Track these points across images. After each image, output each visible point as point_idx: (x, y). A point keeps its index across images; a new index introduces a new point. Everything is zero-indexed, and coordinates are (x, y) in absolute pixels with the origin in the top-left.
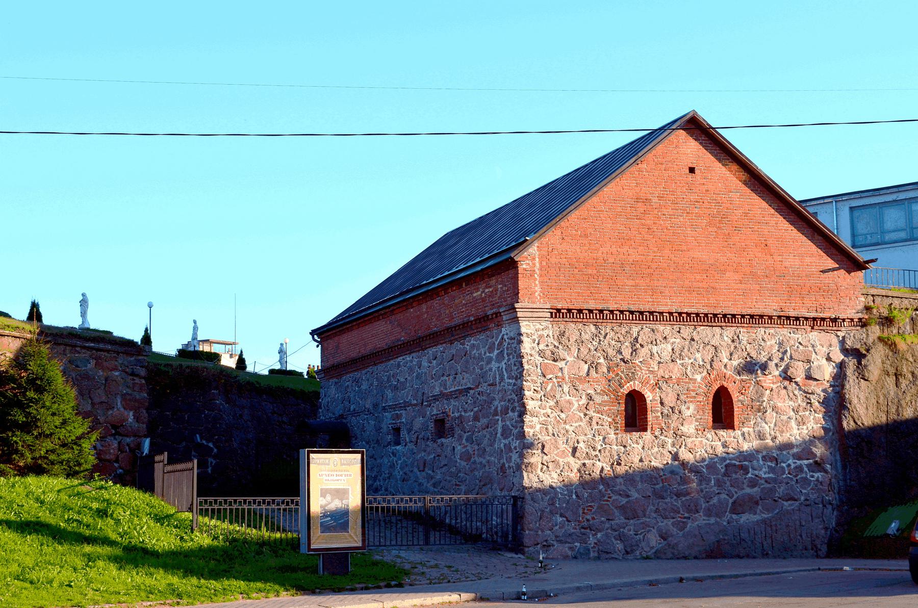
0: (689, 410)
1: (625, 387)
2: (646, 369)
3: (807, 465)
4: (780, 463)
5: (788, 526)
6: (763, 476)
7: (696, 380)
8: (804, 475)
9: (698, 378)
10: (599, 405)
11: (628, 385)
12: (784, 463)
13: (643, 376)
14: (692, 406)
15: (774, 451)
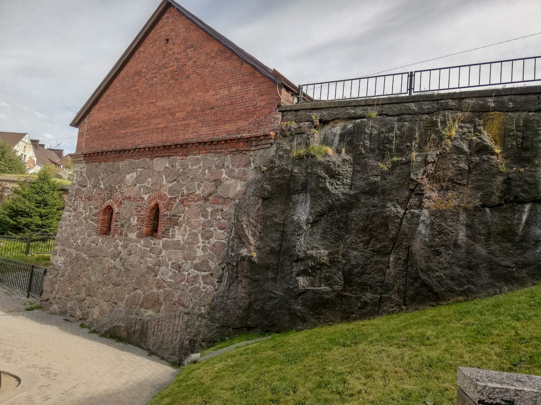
0: (134, 221)
2: (119, 191)
3: (204, 277)
4: (183, 271)
7: (144, 198)
8: (197, 285)
9: (146, 197)
10: (93, 215)
12: (187, 271)
15: (180, 260)
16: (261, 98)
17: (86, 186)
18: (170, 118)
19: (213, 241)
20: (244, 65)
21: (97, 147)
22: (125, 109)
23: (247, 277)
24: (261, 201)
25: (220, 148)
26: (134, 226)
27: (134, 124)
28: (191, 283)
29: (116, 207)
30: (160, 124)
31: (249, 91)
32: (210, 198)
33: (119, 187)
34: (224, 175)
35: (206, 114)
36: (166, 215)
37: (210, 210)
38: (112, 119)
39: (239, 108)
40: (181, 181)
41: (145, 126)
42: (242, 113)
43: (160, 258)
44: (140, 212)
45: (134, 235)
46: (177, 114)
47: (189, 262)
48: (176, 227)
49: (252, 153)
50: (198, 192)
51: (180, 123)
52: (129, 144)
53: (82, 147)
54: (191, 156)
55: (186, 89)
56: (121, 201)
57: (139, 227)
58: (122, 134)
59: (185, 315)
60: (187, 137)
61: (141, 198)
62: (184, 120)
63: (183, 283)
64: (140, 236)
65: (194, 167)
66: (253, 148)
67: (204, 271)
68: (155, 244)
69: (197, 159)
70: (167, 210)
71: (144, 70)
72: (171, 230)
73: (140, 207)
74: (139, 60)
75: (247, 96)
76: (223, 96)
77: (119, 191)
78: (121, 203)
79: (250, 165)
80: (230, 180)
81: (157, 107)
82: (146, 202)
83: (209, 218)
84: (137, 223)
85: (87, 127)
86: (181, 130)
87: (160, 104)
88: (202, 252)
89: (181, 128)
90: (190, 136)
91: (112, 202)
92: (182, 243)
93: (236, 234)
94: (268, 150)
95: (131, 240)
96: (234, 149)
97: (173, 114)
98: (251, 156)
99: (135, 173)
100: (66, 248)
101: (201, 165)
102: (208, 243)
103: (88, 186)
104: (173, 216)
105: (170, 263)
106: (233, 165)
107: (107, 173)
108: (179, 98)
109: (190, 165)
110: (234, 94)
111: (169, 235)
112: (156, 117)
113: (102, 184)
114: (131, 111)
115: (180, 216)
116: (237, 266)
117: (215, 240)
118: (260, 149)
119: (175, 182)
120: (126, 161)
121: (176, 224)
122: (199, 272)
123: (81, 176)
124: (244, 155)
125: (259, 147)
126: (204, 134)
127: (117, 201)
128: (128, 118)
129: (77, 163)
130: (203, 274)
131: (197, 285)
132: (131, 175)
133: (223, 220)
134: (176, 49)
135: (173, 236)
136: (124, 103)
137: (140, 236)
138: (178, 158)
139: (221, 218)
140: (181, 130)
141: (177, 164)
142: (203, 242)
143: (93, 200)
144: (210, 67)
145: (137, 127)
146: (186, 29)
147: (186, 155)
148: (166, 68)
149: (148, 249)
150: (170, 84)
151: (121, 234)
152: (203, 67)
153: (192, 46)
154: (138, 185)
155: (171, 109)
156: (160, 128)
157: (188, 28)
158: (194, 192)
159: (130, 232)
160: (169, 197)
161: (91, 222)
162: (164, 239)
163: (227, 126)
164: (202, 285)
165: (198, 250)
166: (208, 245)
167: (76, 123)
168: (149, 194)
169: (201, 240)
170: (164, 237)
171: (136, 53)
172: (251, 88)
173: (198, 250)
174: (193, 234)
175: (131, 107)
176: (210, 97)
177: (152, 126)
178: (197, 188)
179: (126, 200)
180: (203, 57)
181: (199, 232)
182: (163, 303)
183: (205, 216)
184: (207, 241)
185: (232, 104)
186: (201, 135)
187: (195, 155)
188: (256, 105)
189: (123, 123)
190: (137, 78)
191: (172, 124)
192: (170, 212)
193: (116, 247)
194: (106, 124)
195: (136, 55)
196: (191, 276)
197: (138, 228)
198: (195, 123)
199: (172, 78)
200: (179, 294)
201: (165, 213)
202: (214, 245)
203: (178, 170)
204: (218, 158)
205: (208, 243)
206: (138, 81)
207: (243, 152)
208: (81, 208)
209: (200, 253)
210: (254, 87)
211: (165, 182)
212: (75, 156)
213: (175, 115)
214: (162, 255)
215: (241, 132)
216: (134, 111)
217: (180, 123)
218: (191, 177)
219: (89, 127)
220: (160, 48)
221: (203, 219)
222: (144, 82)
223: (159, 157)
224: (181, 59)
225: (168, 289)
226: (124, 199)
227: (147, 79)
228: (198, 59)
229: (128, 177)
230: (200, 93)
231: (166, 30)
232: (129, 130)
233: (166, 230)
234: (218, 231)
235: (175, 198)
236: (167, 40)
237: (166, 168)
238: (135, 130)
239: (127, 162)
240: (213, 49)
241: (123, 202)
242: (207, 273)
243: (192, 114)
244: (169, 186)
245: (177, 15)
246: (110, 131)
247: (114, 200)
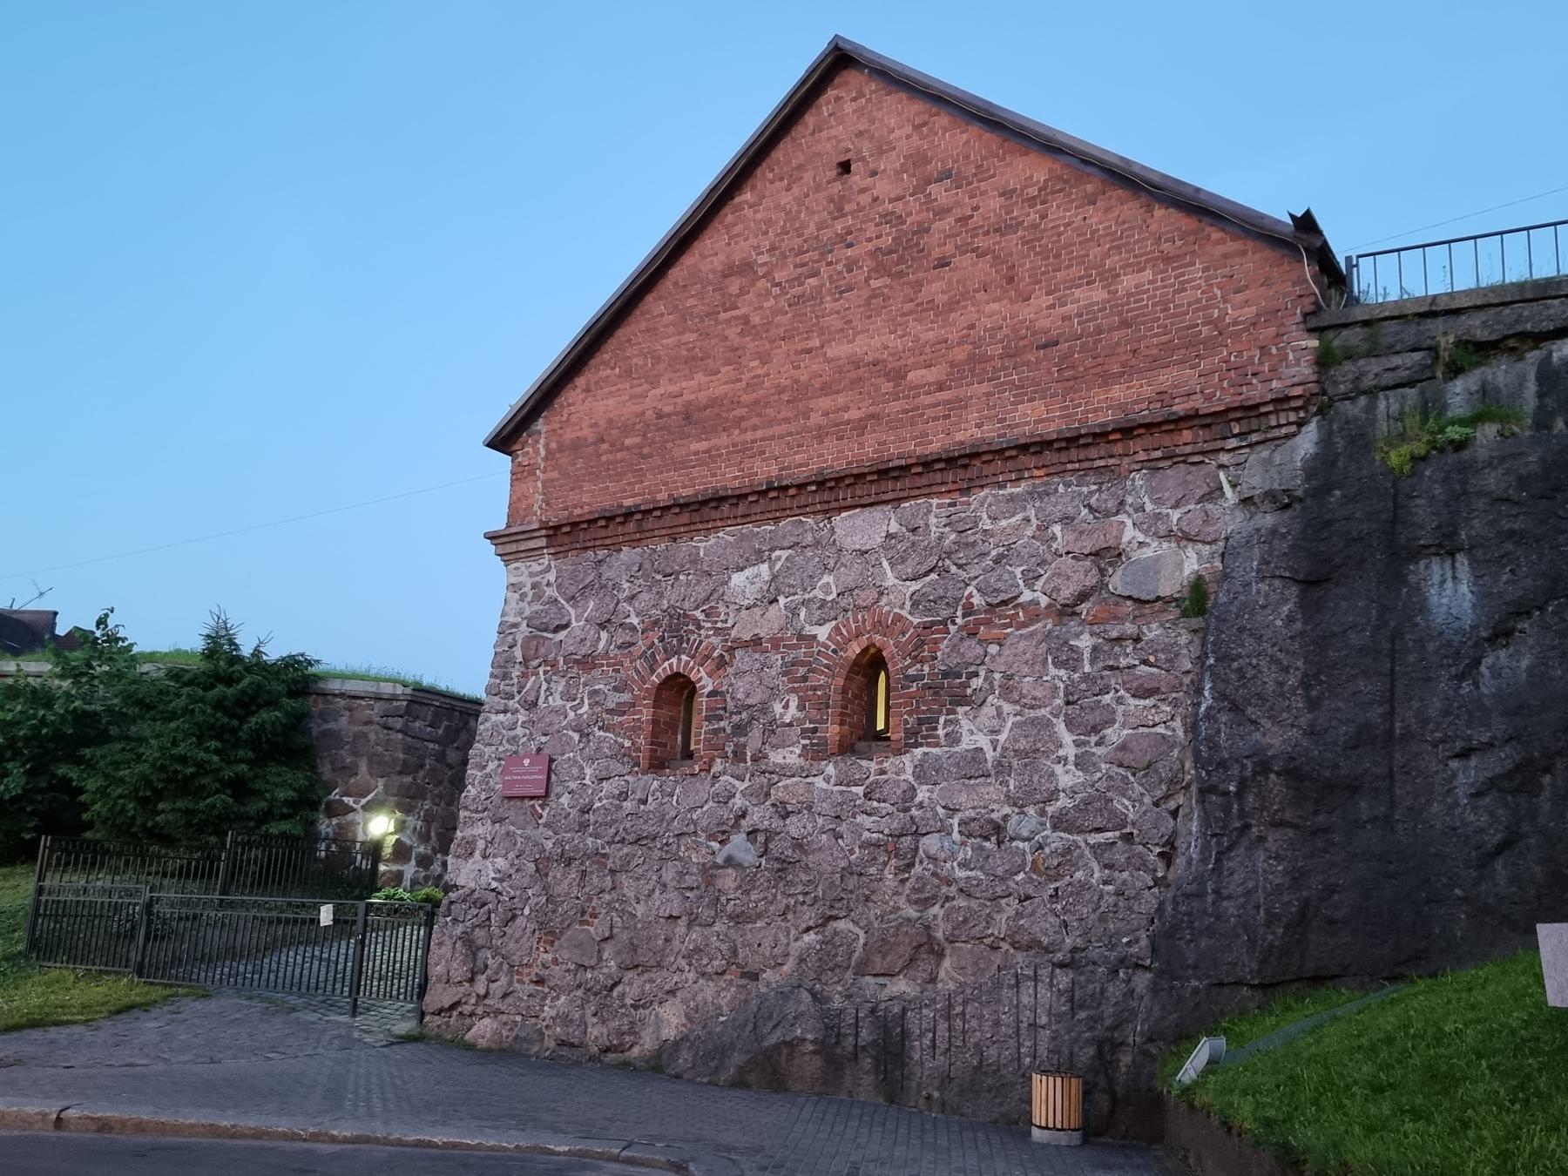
0: (788, 710)
1: (660, 670)
2: (709, 625)
4: (1012, 839)
5: (997, 1023)
6: (961, 874)
8: (1079, 875)
10: (610, 712)
11: (666, 664)
13: (701, 642)
14: (794, 704)
15: (995, 806)
16: (1239, 297)
17: (566, 626)
18: (887, 387)
19: (1114, 734)
20: (1159, 212)
21: (590, 499)
22: (700, 378)
23: (1278, 824)
24: (1294, 590)
25: (1102, 453)
26: (790, 725)
27: (742, 418)
28: (1051, 873)
29: (703, 673)
30: (846, 409)
31: (1188, 281)
32: (1084, 608)
33: (707, 615)
34: (1130, 533)
35: (1028, 364)
36: (914, 679)
37: (1085, 642)
38: (649, 413)
39: (1156, 335)
40: (953, 569)
41: (787, 420)
42: (1168, 347)
43: (914, 812)
44: (805, 679)
45: (791, 752)
46: (911, 375)
47: (1031, 810)
48: (960, 710)
49: (1224, 458)
50: (1027, 596)
51: (929, 400)
52: (728, 477)
53: (530, 506)
54: (986, 491)
55: (941, 299)
56: (721, 656)
57: (807, 725)
58: (696, 453)
59: (1058, 971)
60: (959, 437)
61: (801, 637)
62: (941, 389)
63: (1021, 876)
64: (817, 752)
65: (1004, 523)
66: (1232, 443)
67: (1099, 830)
68: (883, 772)
69: (1012, 498)
70: (918, 660)
71: (762, 259)
72: (942, 720)
73: (803, 664)
74: (736, 230)
75: (1184, 298)
76: (1086, 307)
77: (709, 625)
78: (722, 663)
79: (1223, 494)
80: (1155, 544)
81: (830, 361)
82: (827, 647)
83: (1087, 669)
84: (799, 715)
85: (547, 446)
86: (935, 419)
87: (839, 350)
88: (1081, 773)
89: (930, 412)
90: (970, 431)
91: (687, 663)
92: (990, 755)
93: (1220, 696)
94: (1291, 443)
95: (784, 772)
96: (1158, 454)
97: (898, 376)
98: (1221, 466)
99: (764, 567)
100: (512, 828)
101: (1032, 513)
102: (1098, 744)
103: (574, 624)
104: (945, 675)
105: (955, 821)
106: (1157, 502)
107: (646, 577)
108: (914, 327)
109: (985, 516)
110: (1129, 295)
111: (938, 737)
112: (826, 390)
113: (633, 615)
114: (726, 383)
115: (976, 674)
116: (1240, 794)
117: (1126, 732)
118: (1257, 443)
119: (934, 576)
120: (721, 534)
121: (963, 700)
122: (1079, 838)
123: (538, 597)
124: (1193, 468)
125: (1254, 438)
126: (1027, 423)
127: (707, 657)
128: (714, 402)
129: (517, 560)
130: (1094, 838)
131: (1079, 875)
132: (749, 572)
133: (1143, 667)
134: (882, 188)
135: (953, 739)
136: (692, 361)
137: (817, 752)
138: (935, 501)
139: (1137, 662)
140: (935, 419)
141: (933, 520)
142: (1077, 744)
143: (602, 665)
144: (1026, 229)
145: (755, 428)
146: (917, 128)
147: (966, 491)
148: (850, 246)
149: (859, 790)
150: (874, 290)
151: (739, 756)
152: (996, 231)
153: (948, 175)
154: (782, 600)
155: (884, 361)
156: (848, 422)
157: (925, 124)
158: (1016, 598)
159: (775, 747)
160: (916, 621)
161: (601, 733)
162: (918, 752)
163: (1118, 392)
164: (1096, 875)
165: (1059, 769)
166: (1100, 751)
167: (504, 440)
168: (834, 623)
169: (1067, 738)
170: (917, 745)
171: (727, 209)
172: (1196, 272)
173: (1059, 769)
174: (1033, 722)
175: (724, 370)
176: (1039, 312)
177: (816, 418)
178: (1021, 582)
179: (739, 653)
180: (995, 203)
181: (1057, 716)
182: (948, 952)
183: (1070, 661)
184: (1094, 739)
185: (1125, 324)
186: (1017, 426)
187: (1002, 486)
188: (1221, 318)
189: (691, 418)
190: (734, 286)
191: (895, 406)
192: (932, 668)
193: (726, 799)
194: (626, 430)
195: (728, 215)
196: (1047, 850)
197: (804, 731)
198: (988, 395)
199: (880, 270)
200: (1011, 912)
201: (911, 672)
202: (1123, 747)
203: (941, 538)
204: (1094, 487)
205: (1098, 744)
206: (743, 291)
207: (1196, 459)
208: (558, 697)
209: (1067, 777)
210: (1205, 270)
211: (891, 580)
212: (513, 538)
213: (904, 377)
214: (917, 800)
215: (1177, 401)
216: (740, 380)
217: (929, 400)
218: (994, 553)
219: (553, 445)
220: (818, 188)
221: (1062, 673)
222: (768, 292)
223: (855, 507)
224: (909, 214)
225: (961, 902)
226: (731, 650)
227: (779, 284)
228: (976, 209)
229: (738, 579)
230: (995, 306)
231: (835, 137)
232: (723, 440)
233: (920, 722)
234: (1132, 701)
235: (944, 623)
236: (845, 167)
237: (889, 536)
238: (749, 436)
239: (725, 536)
240: (1031, 177)
241: (727, 658)
242: (1110, 834)
243: (972, 371)
244: (912, 589)
245: (872, 92)
246: (645, 451)
247: (693, 657)
